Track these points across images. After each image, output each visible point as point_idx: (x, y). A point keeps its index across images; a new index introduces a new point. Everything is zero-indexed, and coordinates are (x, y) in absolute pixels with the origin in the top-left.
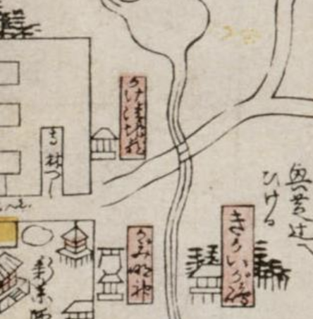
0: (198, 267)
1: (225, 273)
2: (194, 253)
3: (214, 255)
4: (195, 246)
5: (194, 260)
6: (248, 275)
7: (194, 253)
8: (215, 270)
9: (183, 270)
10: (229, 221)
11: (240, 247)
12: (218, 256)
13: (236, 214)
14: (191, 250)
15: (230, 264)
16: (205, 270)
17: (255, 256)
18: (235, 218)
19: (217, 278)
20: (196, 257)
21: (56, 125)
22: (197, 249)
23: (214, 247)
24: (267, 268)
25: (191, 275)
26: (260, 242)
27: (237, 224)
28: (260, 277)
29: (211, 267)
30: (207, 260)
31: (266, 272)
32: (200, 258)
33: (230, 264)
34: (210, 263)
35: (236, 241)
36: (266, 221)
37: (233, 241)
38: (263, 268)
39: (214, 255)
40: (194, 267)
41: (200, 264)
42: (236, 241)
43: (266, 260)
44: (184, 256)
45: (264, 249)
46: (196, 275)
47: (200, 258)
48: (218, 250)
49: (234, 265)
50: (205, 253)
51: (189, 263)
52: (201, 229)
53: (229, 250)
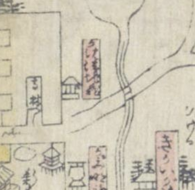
0: (139, 175)
1: (159, 178)
2: (136, 165)
3: (150, 166)
4: (137, 160)
5: (136, 170)
6: (175, 180)
7: (136, 165)
8: (151, 177)
9: (128, 178)
10: (161, 142)
11: (168, 161)
12: (153, 167)
13: (165, 137)
14: (135, 162)
15: (163, 172)
16: (145, 177)
17: (180, 166)
18: (164, 140)
19: (153, 182)
20: (139, 167)
21: (187, 137)
22: (139, 162)
23: (150, 161)
24: (188, 175)
25: (134, 180)
26: (183, 157)
27: (166, 144)
28: (184, 182)
29: (149, 175)
30: (145, 170)
31: (187, 177)
32: (140, 169)
33: (163, 172)
34: (148, 172)
35: (166, 156)
36: (187, 141)
37: (164, 156)
38: (185, 175)
39: (150, 166)
40: (137, 174)
41: (140, 173)
42: (166, 156)
43: (188, 169)
44: (129, 168)
45: (186, 162)
46: (139, 180)
47: (140, 169)
48: (153, 162)
49: (165, 173)
50: (143, 166)
51: (132, 172)
52: (143, 147)
53: (162, 164)
